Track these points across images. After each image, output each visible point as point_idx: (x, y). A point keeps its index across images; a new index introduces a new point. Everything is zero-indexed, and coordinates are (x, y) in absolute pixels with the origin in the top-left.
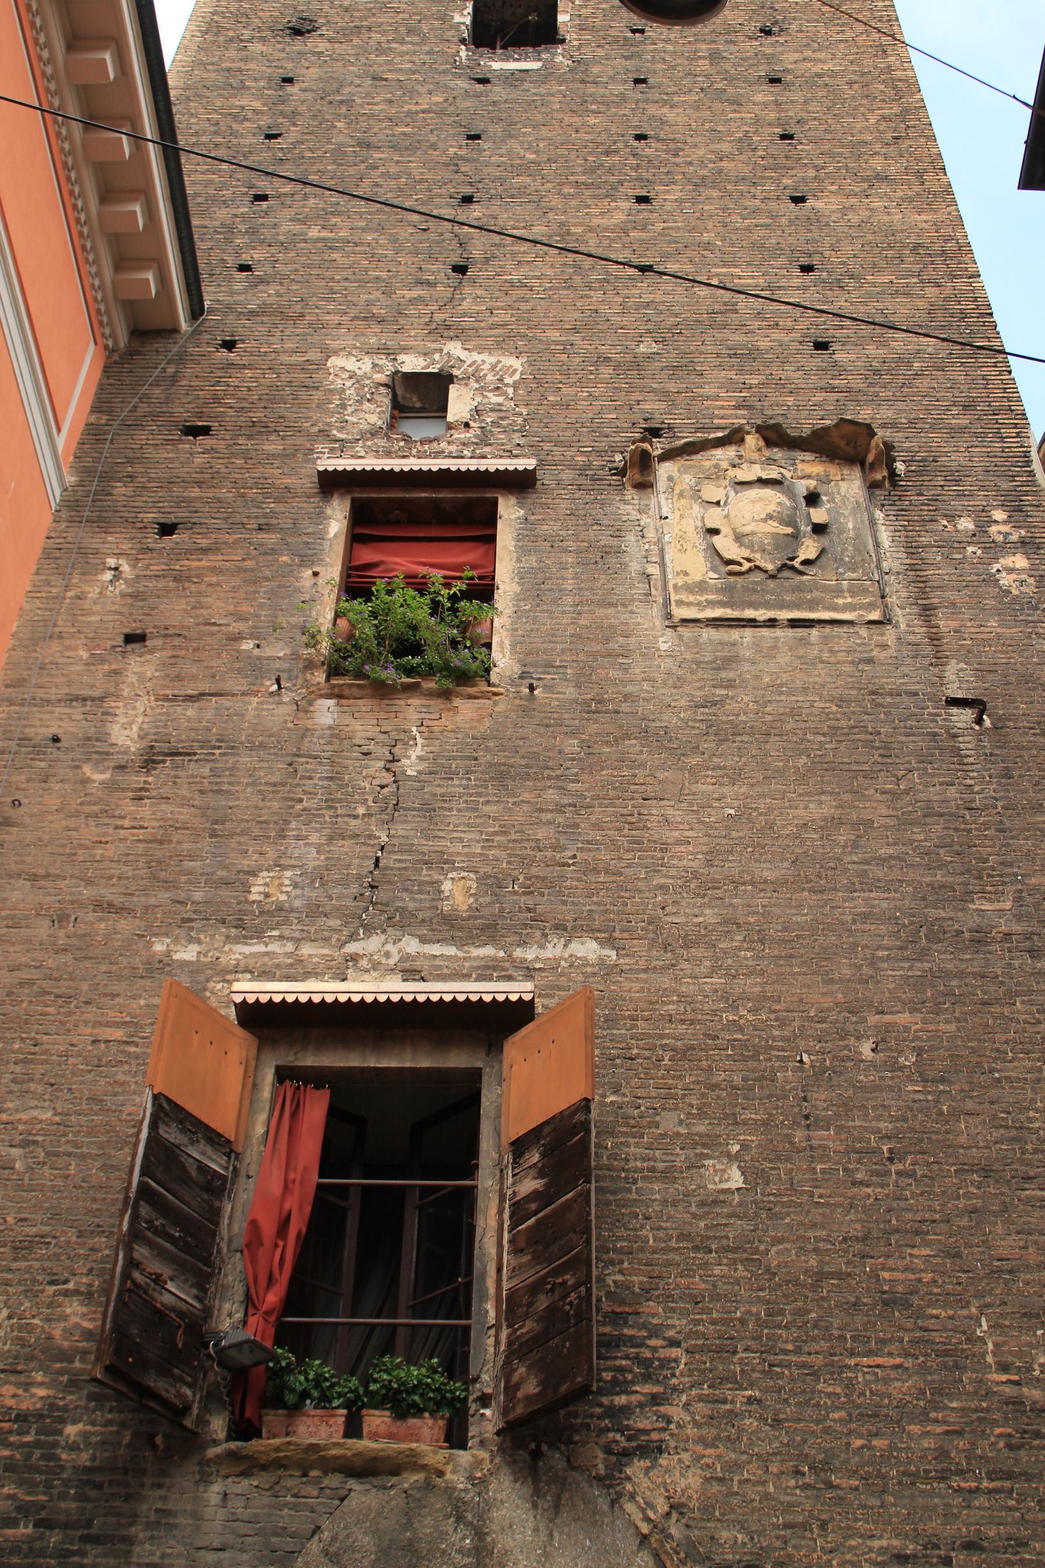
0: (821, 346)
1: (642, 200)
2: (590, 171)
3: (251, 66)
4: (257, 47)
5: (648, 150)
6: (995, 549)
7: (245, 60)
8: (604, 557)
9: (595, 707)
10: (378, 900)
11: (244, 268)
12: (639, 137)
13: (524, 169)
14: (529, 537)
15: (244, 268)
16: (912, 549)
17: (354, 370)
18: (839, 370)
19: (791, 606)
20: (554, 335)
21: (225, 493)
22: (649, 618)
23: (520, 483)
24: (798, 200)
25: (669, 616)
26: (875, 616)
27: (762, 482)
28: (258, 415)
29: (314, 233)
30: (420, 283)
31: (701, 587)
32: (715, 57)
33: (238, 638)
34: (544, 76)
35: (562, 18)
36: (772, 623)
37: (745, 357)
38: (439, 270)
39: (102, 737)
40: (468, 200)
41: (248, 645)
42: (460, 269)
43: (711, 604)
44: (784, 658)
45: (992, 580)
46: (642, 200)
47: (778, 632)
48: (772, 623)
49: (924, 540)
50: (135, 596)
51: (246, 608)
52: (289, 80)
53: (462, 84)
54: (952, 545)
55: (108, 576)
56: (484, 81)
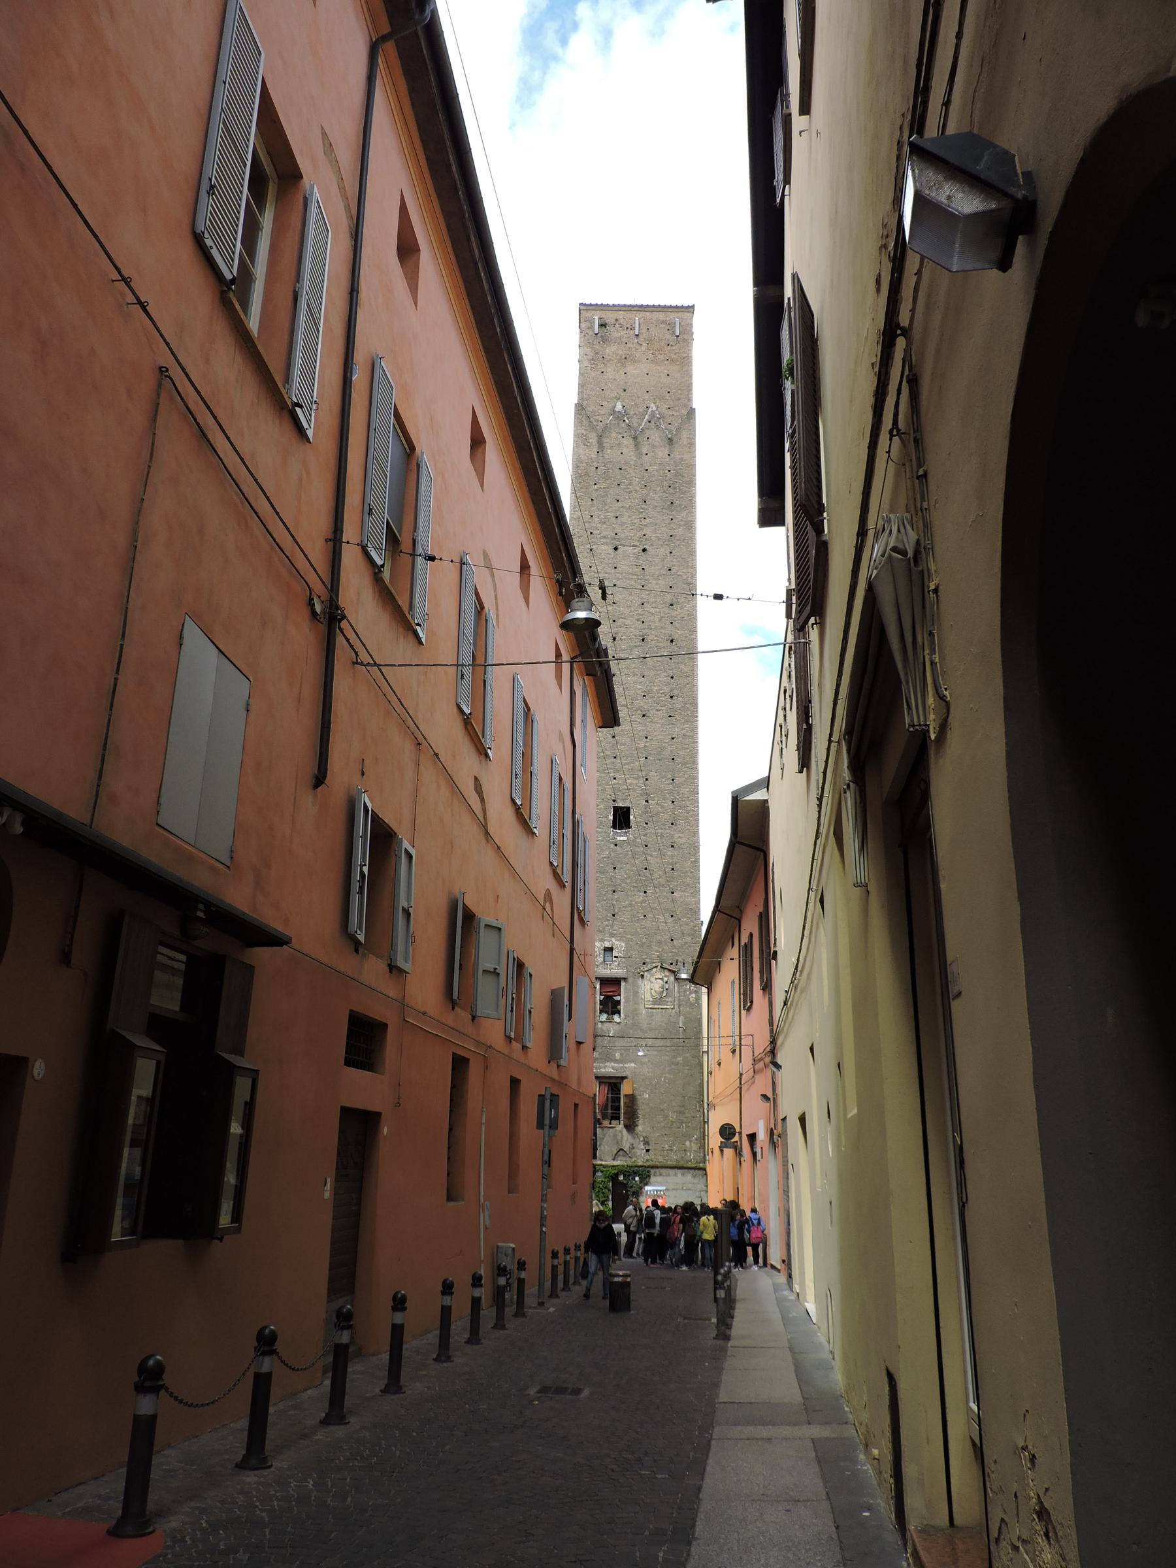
5: (647, 873)
8: (636, 993)
9: (634, 1025)
10: (608, 1058)
13: (623, 881)
14: (625, 988)
17: (599, 945)
18: (674, 946)
22: (642, 1007)
23: (625, 979)
32: (662, 836)
37: (660, 942)
53: (612, 846)
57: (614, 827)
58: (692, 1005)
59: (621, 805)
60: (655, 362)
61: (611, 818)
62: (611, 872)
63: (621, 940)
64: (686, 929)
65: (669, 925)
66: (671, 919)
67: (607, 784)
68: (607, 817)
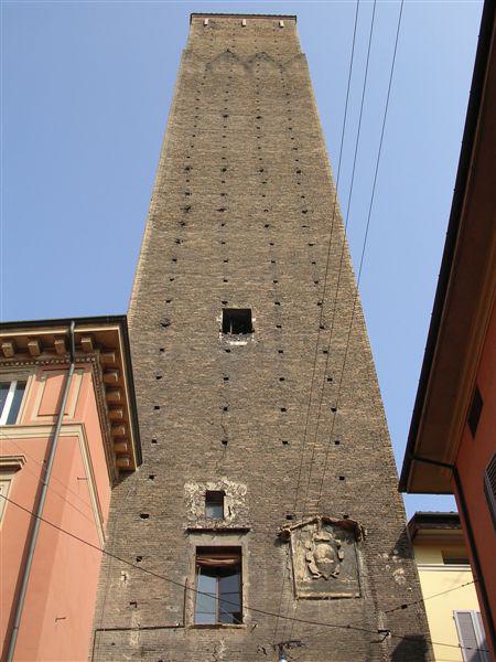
0: (342, 478)
1: (283, 410)
2: (265, 396)
3: (149, 342)
4: (150, 333)
5: (285, 385)
6: (394, 566)
7: (147, 340)
11: (154, 441)
12: (282, 379)
13: (242, 395)
15: (154, 441)
16: (369, 566)
17: (192, 488)
19: (333, 591)
20: (257, 474)
21: (155, 544)
22: (288, 595)
24: (334, 410)
25: (295, 596)
26: (358, 595)
27: (323, 541)
28: (163, 509)
29: (176, 425)
30: (212, 449)
31: (304, 584)
32: (306, 340)
33: (165, 604)
34: (249, 348)
35: (253, 320)
36: (327, 598)
38: (218, 443)
39: (127, 643)
40: (226, 409)
41: (168, 607)
42: (225, 443)
43: (307, 591)
44: (331, 612)
45: (392, 578)
46: (283, 410)
47: (329, 601)
48: (327, 598)
49: (374, 562)
50: (132, 587)
51: (166, 592)
52: (162, 350)
54: (381, 564)
55: (123, 578)
56: (228, 351)
57: (225, 330)
58: (398, 589)
59: (235, 307)
60: (263, 36)
61: (220, 319)
62: (220, 384)
63: (239, 479)
64: (366, 461)
65: (332, 456)
66: (334, 447)
67: (213, 286)
68: (213, 319)
